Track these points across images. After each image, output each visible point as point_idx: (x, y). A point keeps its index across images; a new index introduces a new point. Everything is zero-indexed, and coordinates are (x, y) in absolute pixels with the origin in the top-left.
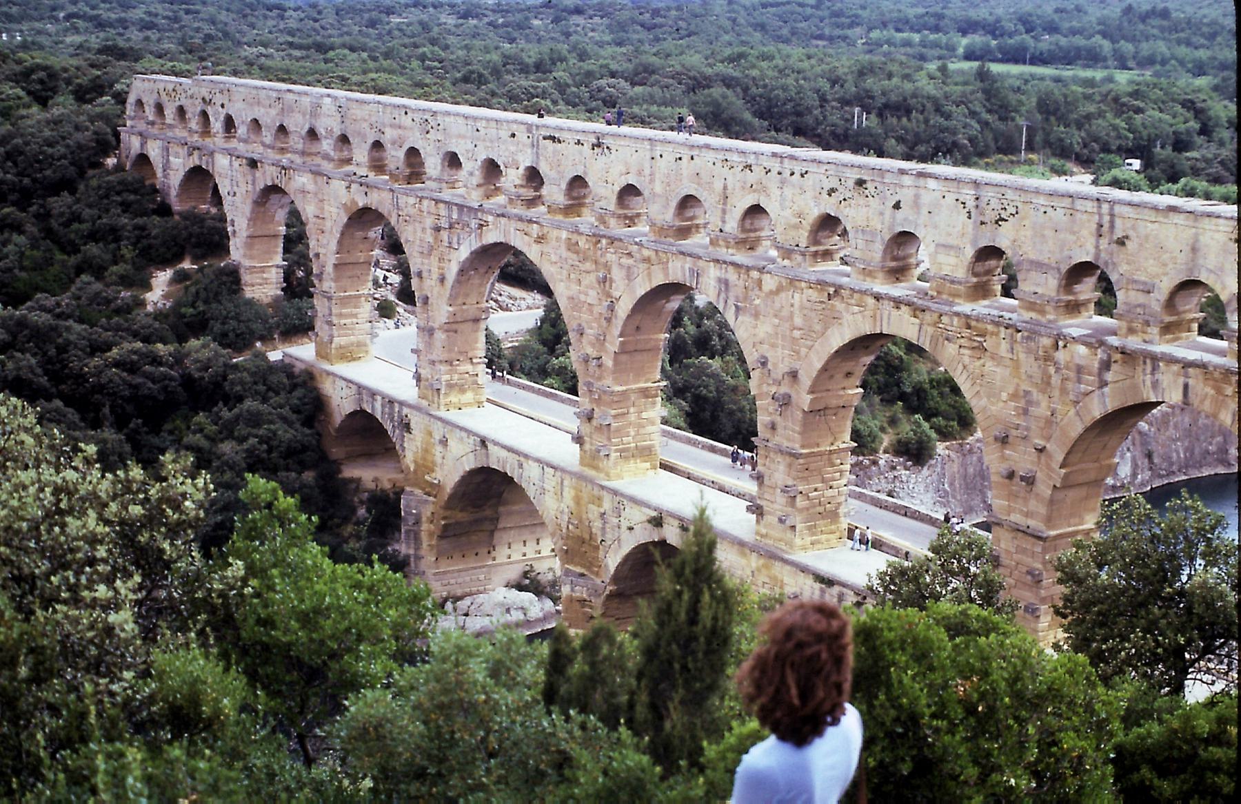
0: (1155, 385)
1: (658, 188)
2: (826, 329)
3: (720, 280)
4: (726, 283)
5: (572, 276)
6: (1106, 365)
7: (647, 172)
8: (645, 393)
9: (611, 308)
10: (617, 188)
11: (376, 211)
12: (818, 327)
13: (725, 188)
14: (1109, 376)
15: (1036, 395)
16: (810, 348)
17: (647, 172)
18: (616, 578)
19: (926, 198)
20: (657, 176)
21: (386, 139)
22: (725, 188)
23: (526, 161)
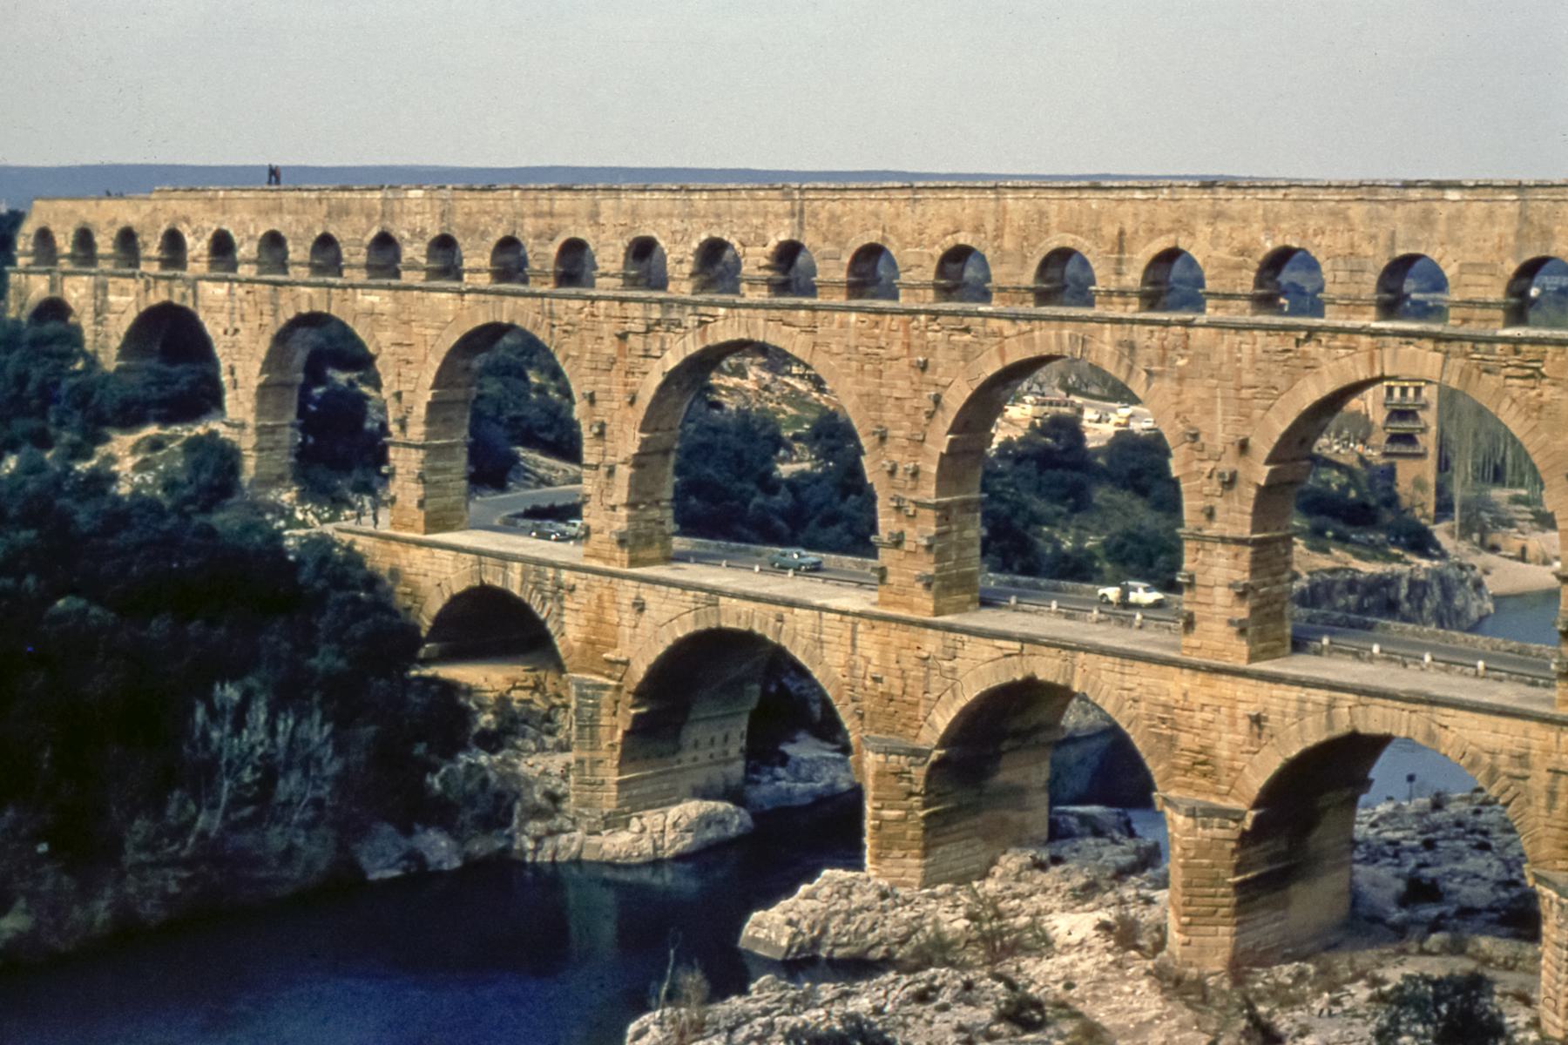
1: (1008, 243)
2: (1293, 382)
3: (1120, 344)
4: (1132, 346)
5: (867, 367)
7: (990, 227)
8: (965, 506)
9: (937, 400)
10: (938, 251)
11: (509, 328)
12: (1282, 383)
16: (1268, 409)
17: (990, 227)
18: (945, 742)
19: (1442, 211)
20: (1007, 230)
21: (527, 231)
22: (1122, 233)
23: (780, 234)
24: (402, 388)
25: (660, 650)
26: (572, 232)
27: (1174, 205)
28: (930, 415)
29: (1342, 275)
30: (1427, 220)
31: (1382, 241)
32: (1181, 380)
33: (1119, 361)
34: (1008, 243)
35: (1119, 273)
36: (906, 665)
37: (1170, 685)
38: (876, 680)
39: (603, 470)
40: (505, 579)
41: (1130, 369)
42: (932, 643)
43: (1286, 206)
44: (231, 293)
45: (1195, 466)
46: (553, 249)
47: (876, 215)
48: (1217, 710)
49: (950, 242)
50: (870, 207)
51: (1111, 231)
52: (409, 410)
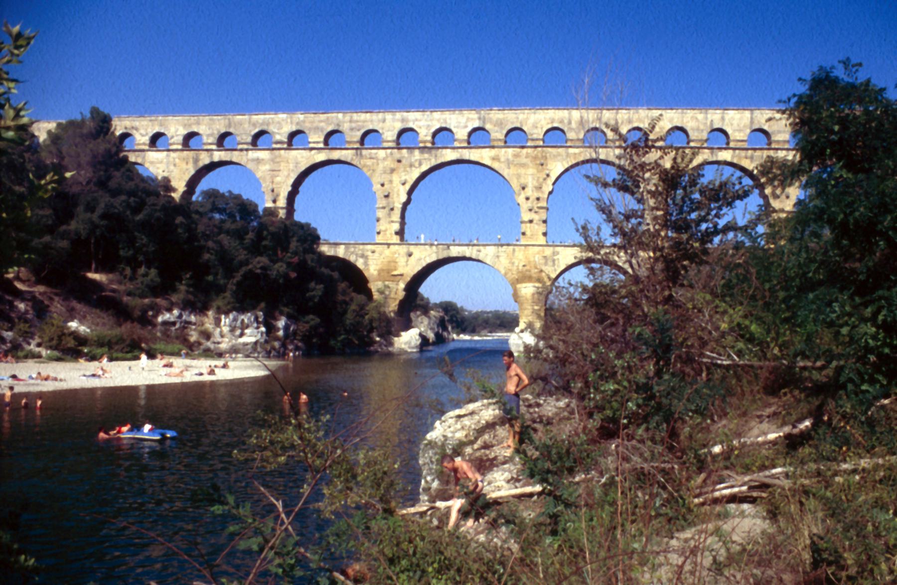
7: (566, 121)
17: (566, 121)
20: (573, 122)
24: (274, 186)
25: (420, 268)
26: (371, 127)
28: (545, 179)
29: (696, 134)
30: (723, 119)
31: (709, 123)
34: (574, 125)
36: (537, 259)
38: (524, 266)
39: (387, 210)
40: (336, 251)
42: (548, 251)
43: (676, 115)
44: (168, 156)
46: (359, 134)
47: (518, 118)
49: (550, 126)
50: (514, 116)
52: (278, 195)
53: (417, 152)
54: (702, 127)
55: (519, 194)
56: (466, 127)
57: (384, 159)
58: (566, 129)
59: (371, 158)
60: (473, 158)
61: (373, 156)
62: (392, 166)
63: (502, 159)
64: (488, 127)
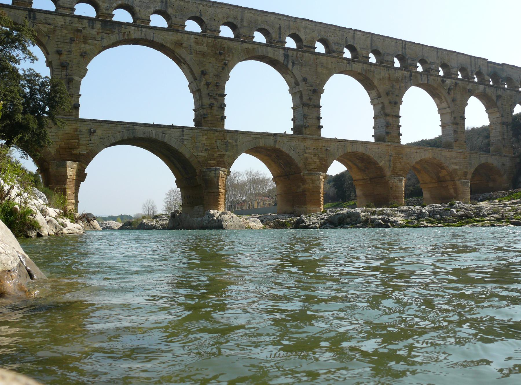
0: (422, 79)
1: (245, 24)
4: (288, 56)
6: (411, 76)
7: (239, 18)
13: (280, 28)
14: (412, 78)
15: (395, 84)
20: (245, 20)
22: (280, 28)
27: (295, 23)
28: (223, 69)
29: (337, 47)
30: (354, 38)
31: (344, 40)
32: (302, 65)
33: (284, 60)
34: (245, 24)
35: (280, 37)
37: (305, 144)
41: (288, 62)
45: (306, 88)
47: (197, 8)
48: (317, 150)
51: (278, 26)
53: (98, 25)
54: (340, 42)
55: (200, 81)
56: (148, 8)
57: (63, 27)
58: (239, 26)
59: (46, 23)
60: (156, 40)
61: (49, 21)
62: (72, 36)
63: (184, 45)
64: (170, 11)
